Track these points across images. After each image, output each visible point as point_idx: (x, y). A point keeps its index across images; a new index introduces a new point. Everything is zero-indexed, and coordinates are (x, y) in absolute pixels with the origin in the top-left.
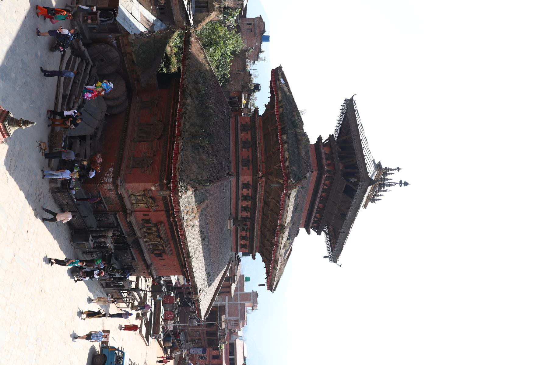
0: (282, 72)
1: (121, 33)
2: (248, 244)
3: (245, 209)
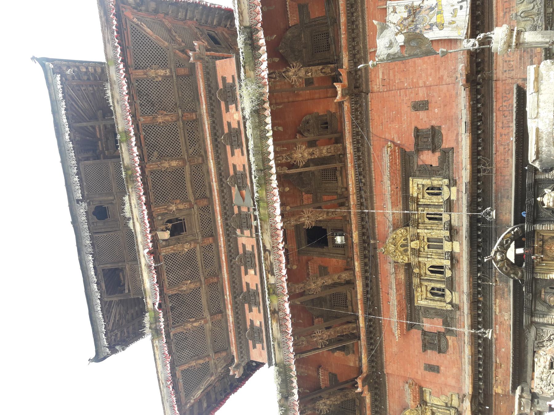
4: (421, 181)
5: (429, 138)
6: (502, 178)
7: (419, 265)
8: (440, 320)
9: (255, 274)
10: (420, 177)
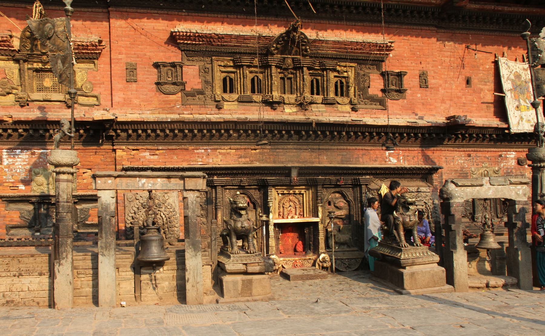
4: (351, 74)
6: (360, 156)
7: (266, 66)
8: (199, 87)
10: (357, 75)
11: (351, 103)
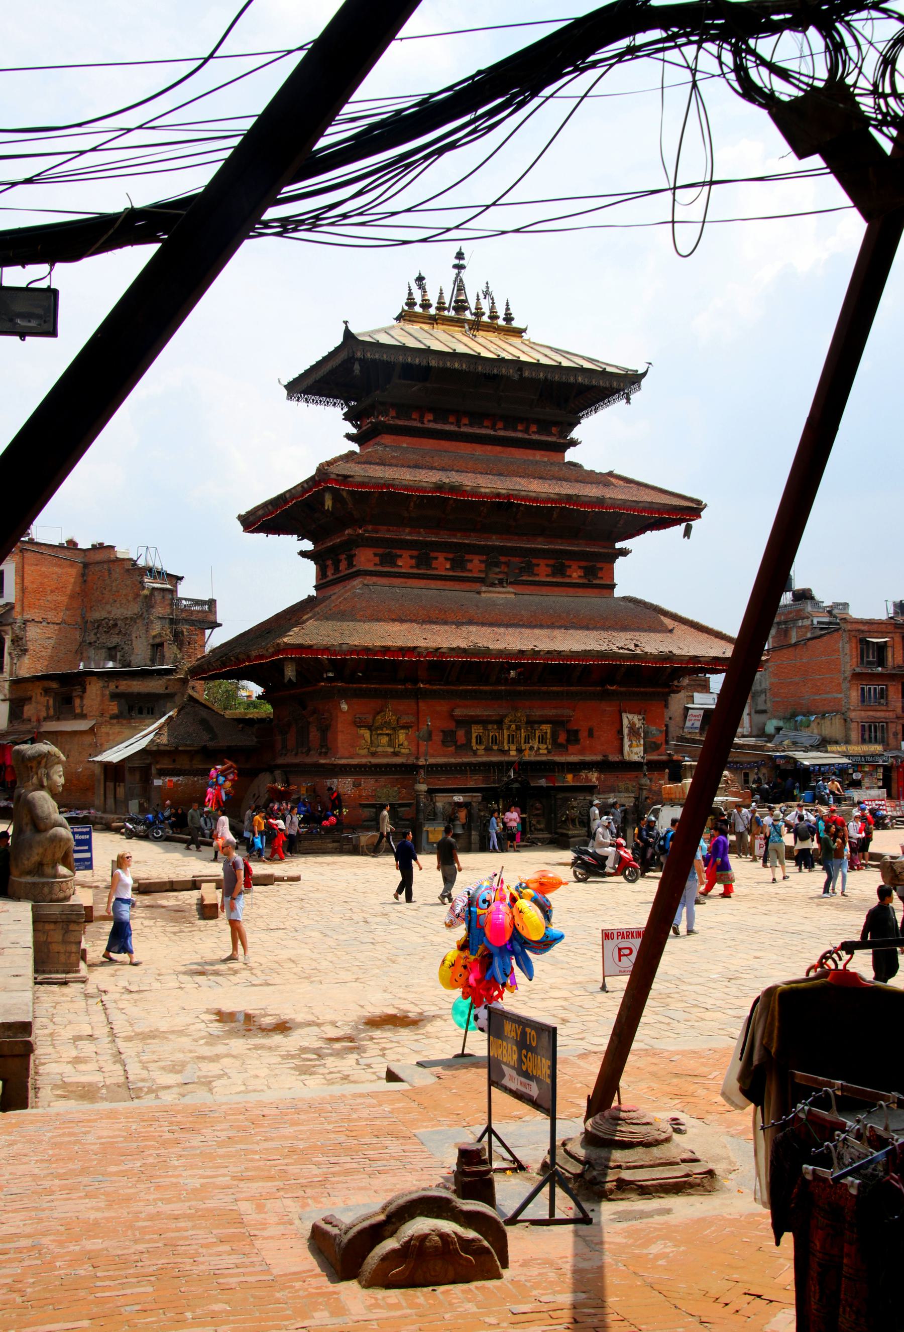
0: (249, 513)
1: (150, 765)
2: (583, 564)
3: (458, 563)
4: (549, 731)
5: (573, 737)
7: (501, 728)
9: (447, 569)
11: (547, 748)
